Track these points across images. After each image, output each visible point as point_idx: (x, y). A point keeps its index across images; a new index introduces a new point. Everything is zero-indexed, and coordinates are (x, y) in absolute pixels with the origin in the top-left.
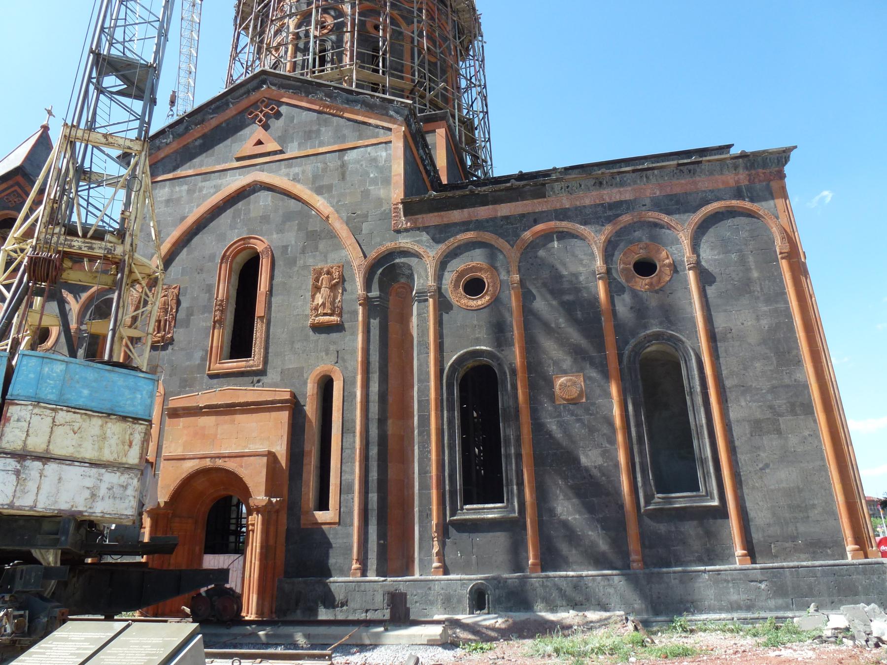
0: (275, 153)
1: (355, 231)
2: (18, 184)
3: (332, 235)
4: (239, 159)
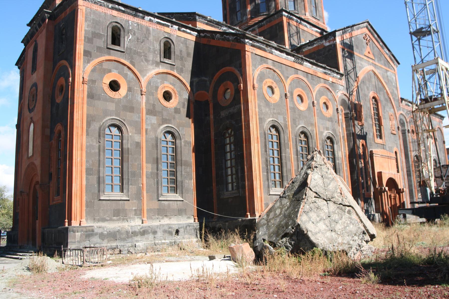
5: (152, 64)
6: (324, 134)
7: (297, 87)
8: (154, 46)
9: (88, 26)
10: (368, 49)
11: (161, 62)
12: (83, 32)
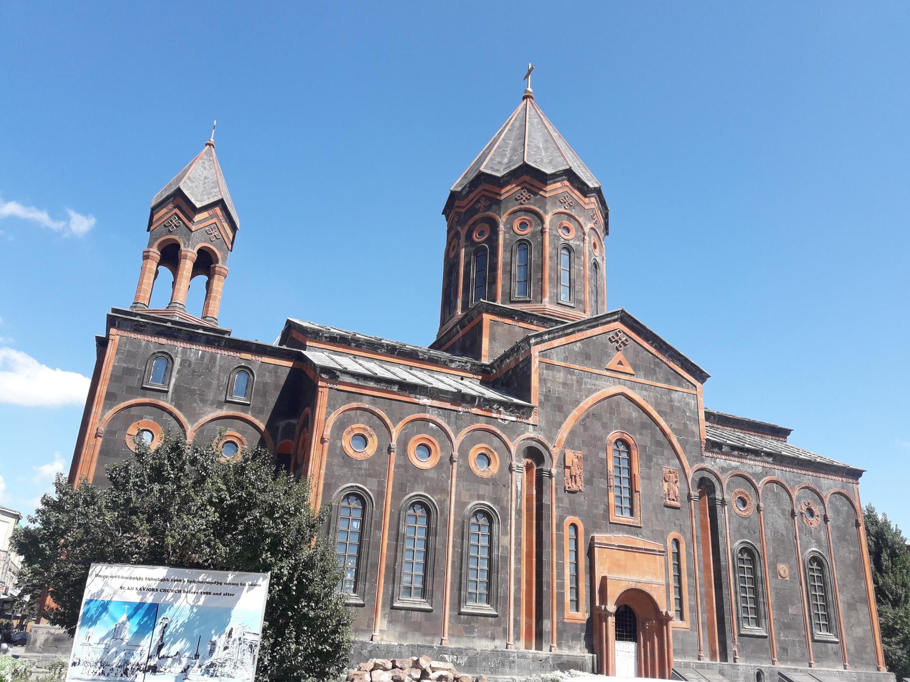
5: (212, 404)
6: (469, 507)
7: (418, 433)
8: (218, 380)
9: (119, 361)
10: (619, 356)
11: (227, 402)
12: (111, 368)
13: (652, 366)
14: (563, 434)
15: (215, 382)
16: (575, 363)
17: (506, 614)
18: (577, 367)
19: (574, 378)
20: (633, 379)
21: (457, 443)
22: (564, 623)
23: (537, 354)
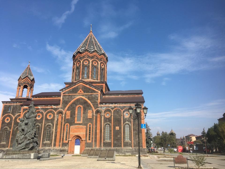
0: (83, 93)
1: (94, 106)
2: (27, 79)
3: (91, 106)
4: (78, 93)
9: (4, 109)
10: (81, 90)
13: (88, 90)
14: (66, 108)
15: (17, 109)
16: (71, 94)
17: (52, 142)
18: (71, 94)
19: (70, 97)
20: (83, 94)
21: (44, 114)
22: (63, 143)
23: (62, 94)
